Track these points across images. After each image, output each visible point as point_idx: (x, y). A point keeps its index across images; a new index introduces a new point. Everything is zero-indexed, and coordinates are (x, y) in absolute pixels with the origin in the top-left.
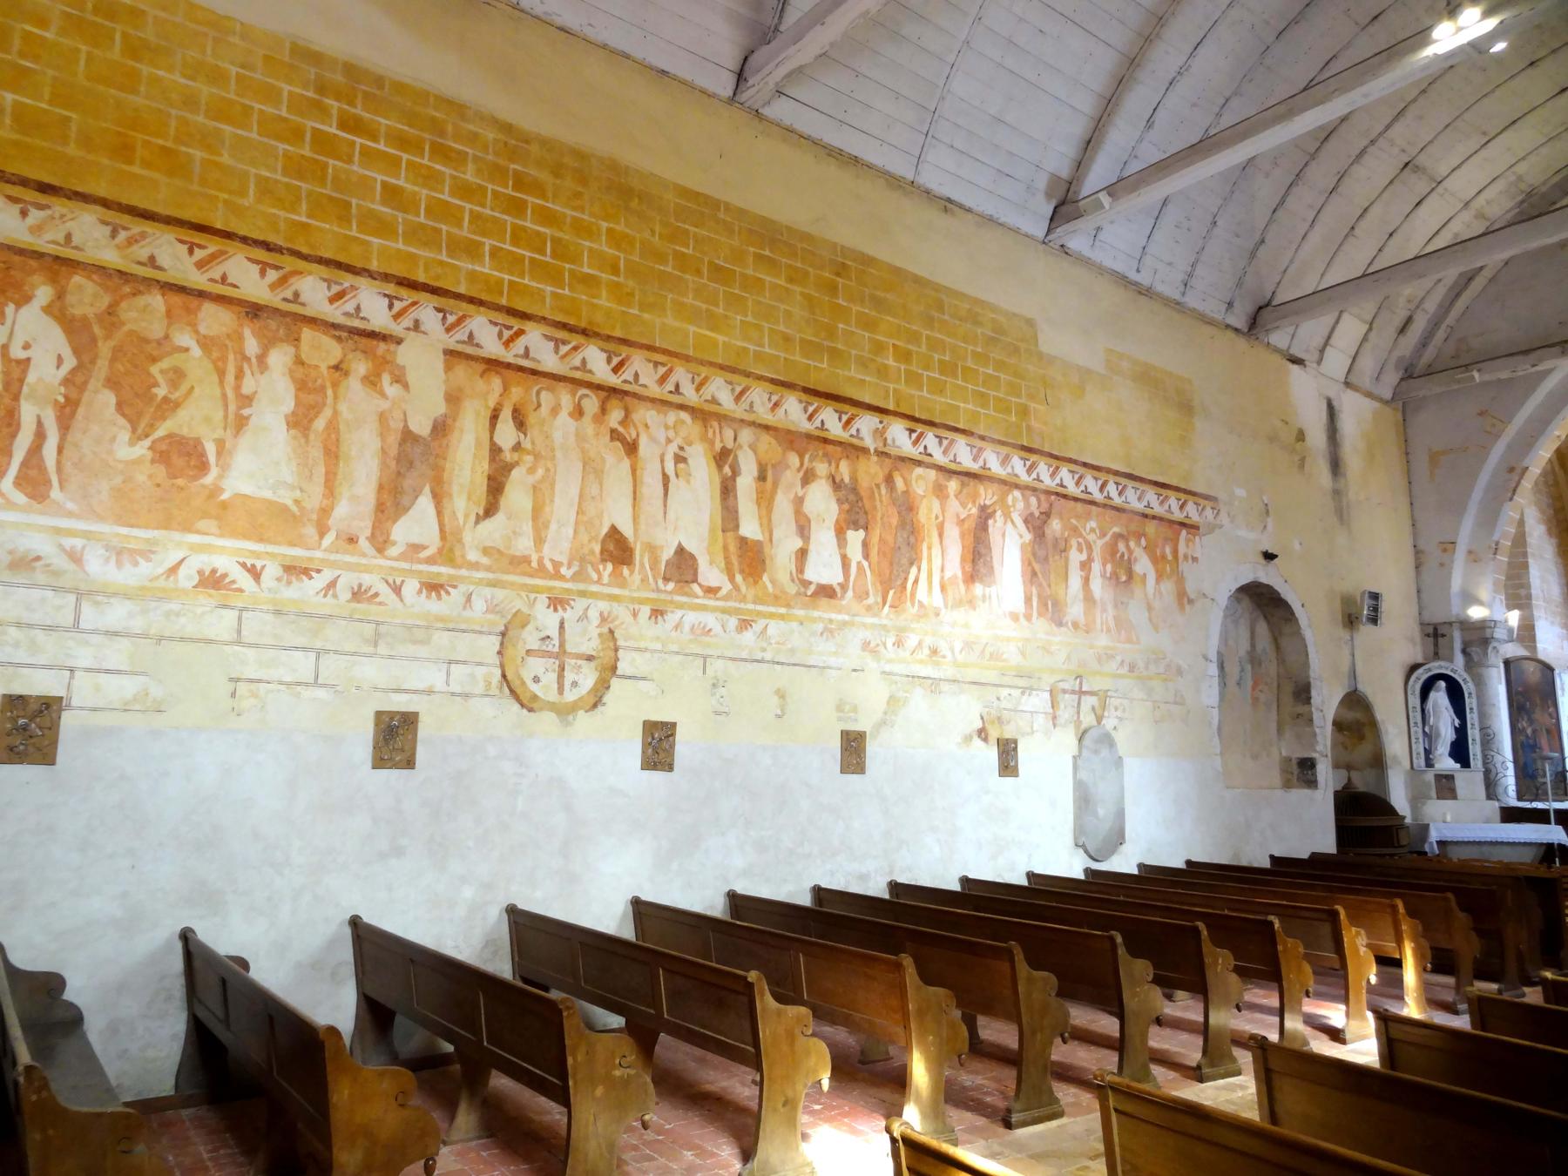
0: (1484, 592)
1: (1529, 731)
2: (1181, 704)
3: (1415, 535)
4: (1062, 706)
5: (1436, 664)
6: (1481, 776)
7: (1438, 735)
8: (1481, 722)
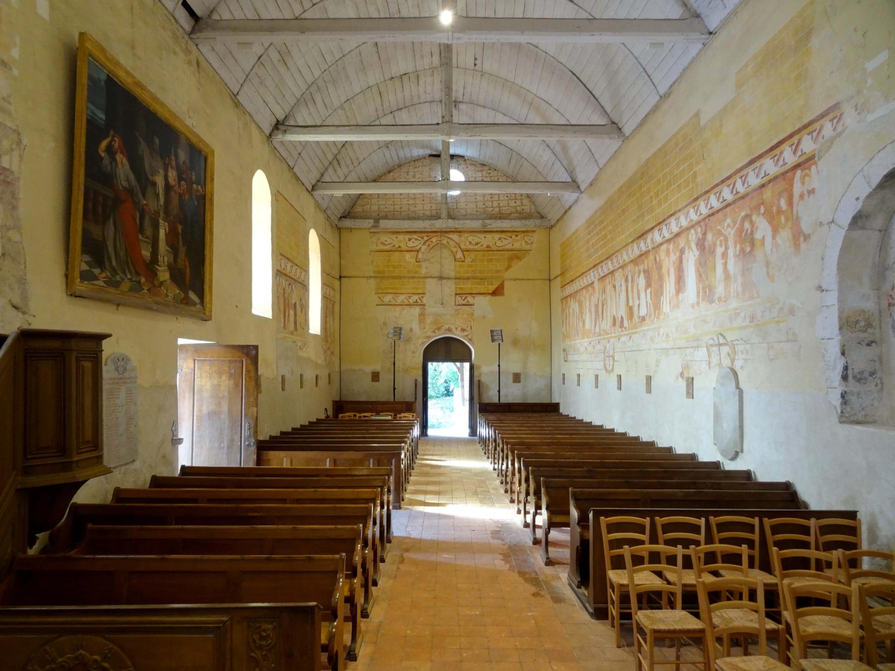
2: (795, 341)
4: (713, 356)
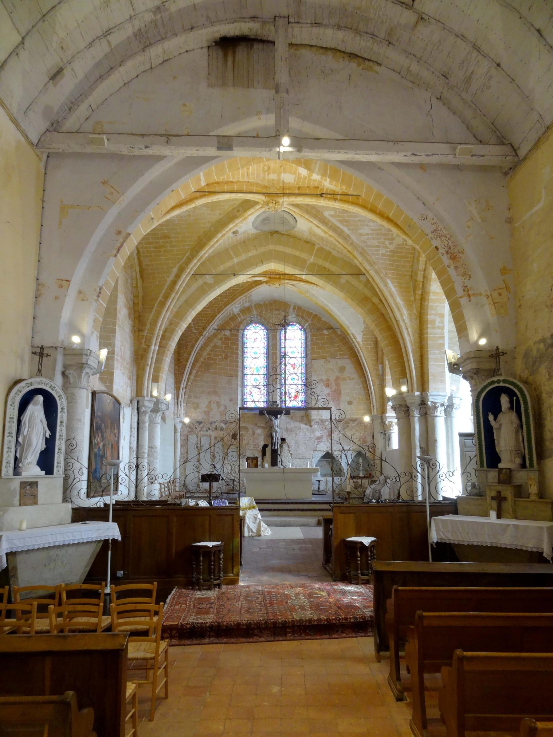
0: (86, 326)
1: (101, 445)
3: (39, 271)
5: (38, 379)
6: (61, 481)
7: (30, 445)
8: (68, 434)
